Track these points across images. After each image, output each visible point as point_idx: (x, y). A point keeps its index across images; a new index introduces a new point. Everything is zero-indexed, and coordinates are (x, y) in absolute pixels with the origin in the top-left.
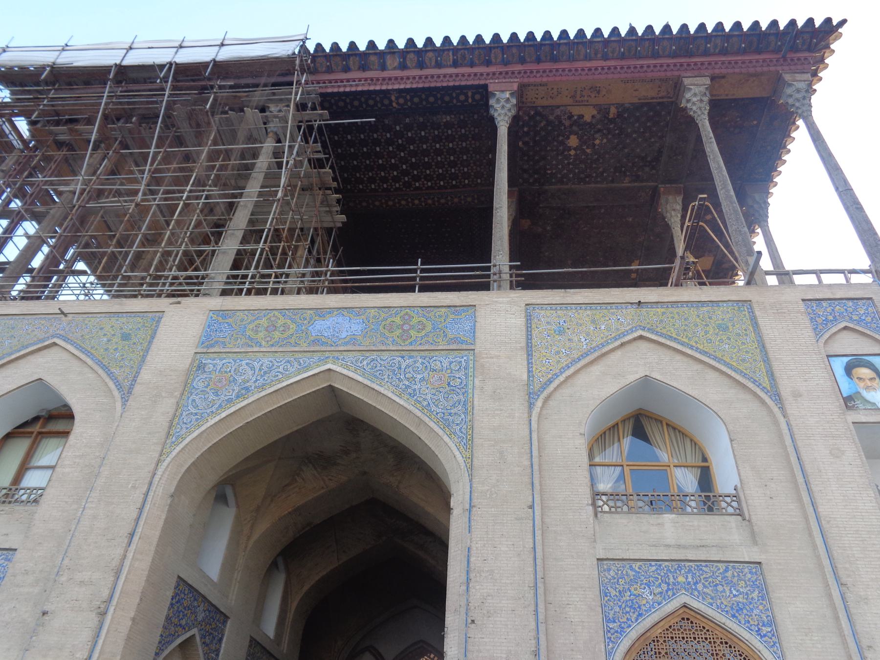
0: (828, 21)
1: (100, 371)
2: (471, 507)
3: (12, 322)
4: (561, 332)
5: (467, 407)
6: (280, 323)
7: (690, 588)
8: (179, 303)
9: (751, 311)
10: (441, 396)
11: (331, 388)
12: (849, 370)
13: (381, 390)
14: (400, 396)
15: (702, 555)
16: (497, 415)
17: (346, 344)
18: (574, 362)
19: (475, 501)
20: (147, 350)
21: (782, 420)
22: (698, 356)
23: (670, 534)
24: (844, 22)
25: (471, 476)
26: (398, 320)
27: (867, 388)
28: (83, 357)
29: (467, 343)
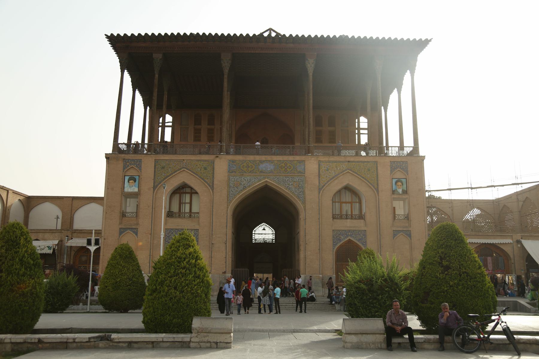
0: (427, 39)
5: (304, 192)
6: (250, 164)
7: (351, 236)
9: (377, 165)
10: (297, 190)
11: (266, 185)
12: (396, 183)
15: (354, 229)
16: (311, 195)
17: (270, 173)
18: (331, 180)
20: (213, 173)
23: (348, 224)
26: (283, 164)
27: (399, 188)
29: (301, 173)
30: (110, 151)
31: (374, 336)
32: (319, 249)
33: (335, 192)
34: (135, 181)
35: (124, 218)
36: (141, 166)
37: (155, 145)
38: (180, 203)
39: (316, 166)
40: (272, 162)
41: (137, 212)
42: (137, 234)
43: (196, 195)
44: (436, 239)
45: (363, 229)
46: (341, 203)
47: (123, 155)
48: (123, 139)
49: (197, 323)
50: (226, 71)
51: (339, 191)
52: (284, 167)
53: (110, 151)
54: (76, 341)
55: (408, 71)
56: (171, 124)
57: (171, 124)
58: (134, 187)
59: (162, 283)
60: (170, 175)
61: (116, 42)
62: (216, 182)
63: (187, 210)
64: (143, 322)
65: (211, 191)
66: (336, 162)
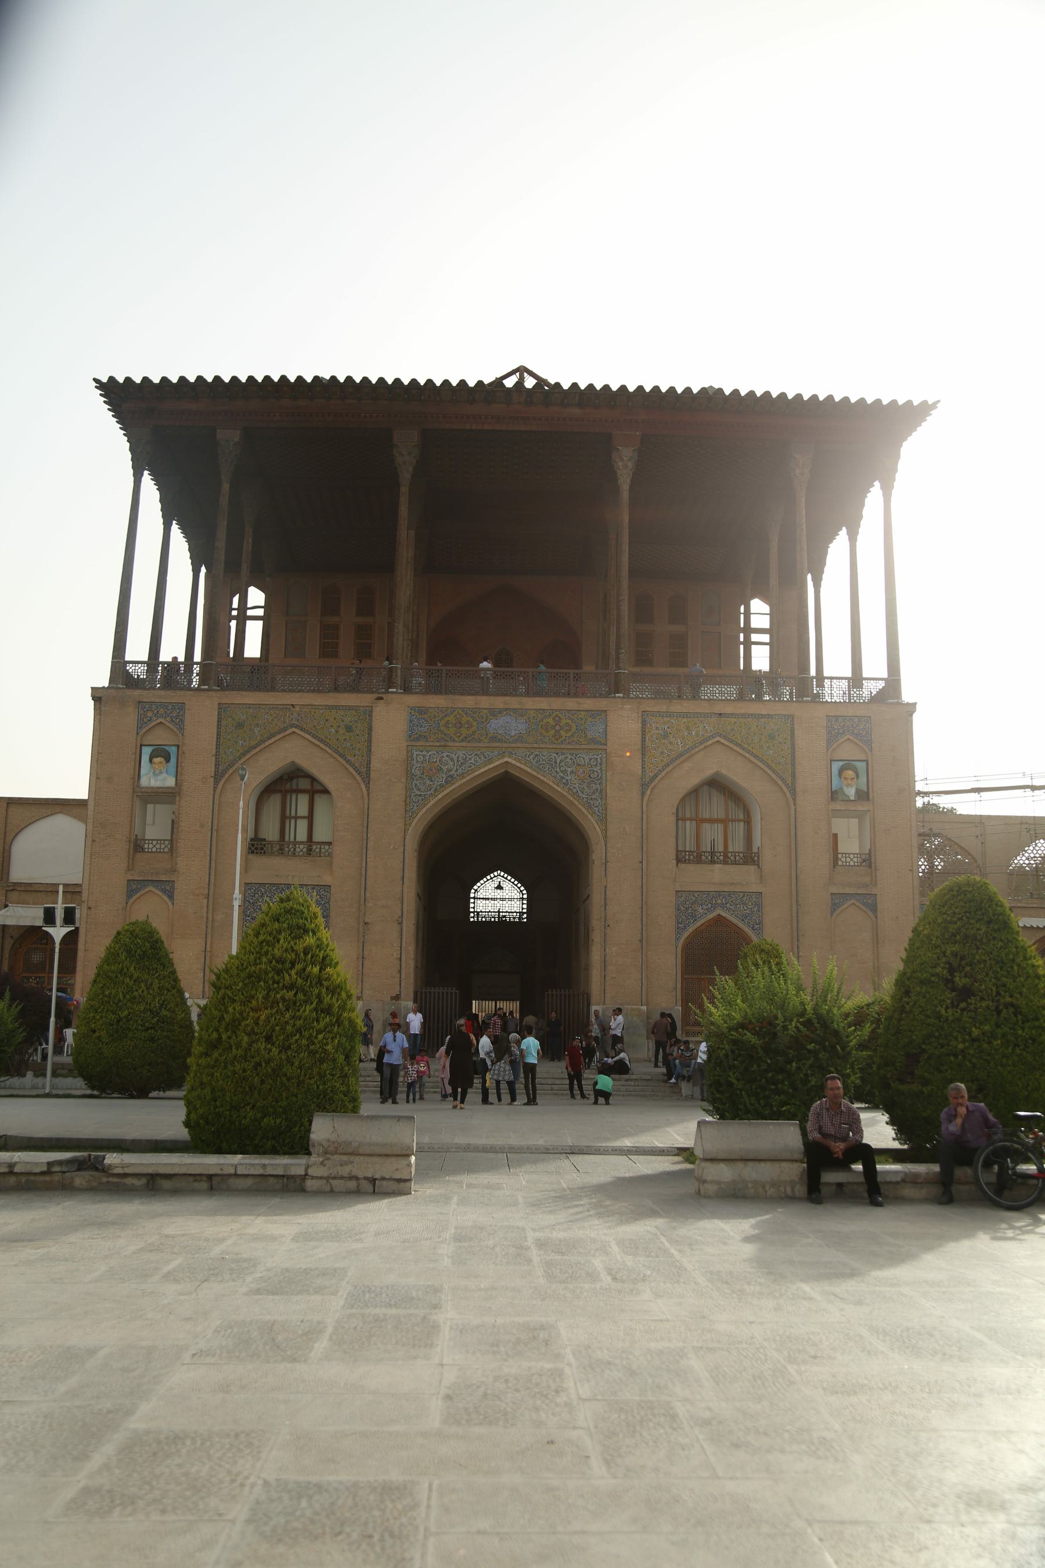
0: (925, 402)
1: (340, 759)
2: (606, 862)
3: (251, 711)
4: (665, 736)
5: (603, 794)
6: (465, 719)
7: (723, 906)
8: (381, 698)
11: (506, 772)
13: (545, 779)
14: (557, 785)
16: (622, 800)
18: (672, 761)
19: (609, 859)
20: (370, 741)
21: (793, 807)
22: (752, 758)
24: (938, 401)
25: (606, 842)
26: (550, 721)
27: (848, 785)
28: (322, 745)
30: (104, 681)
31: (777, 1164)
32: (641, 941)
33: (683, 792)
34: (168, 760)
35: (138, 856)
36: (182, 721)
37: (220, 666)
38: (284, 818)
39: (636, 726)
40: (520, 713)
41: (171, 841)
42: (171, 897)
43: (324, 796)
44: (939, 920)
45: (755, 888)
46: (699, 821)
47: (137, 692)
48: (137, 650)
49: (322, 1129)
50: (406, 476)
51: (695, 793)
52: (553, 727)
53: (104, 681)
54: (17, 1169)
55: (877, 484)
56: (260, 612)
57: (260, 612)
58: (165, 775)
59: (234, 1026)
60: (258, 745)
61: (123, 397)
62: (375, 764)
63: (302, 835)
64: (187, 1124)
65: (363, 787)
66: (686, 715)
